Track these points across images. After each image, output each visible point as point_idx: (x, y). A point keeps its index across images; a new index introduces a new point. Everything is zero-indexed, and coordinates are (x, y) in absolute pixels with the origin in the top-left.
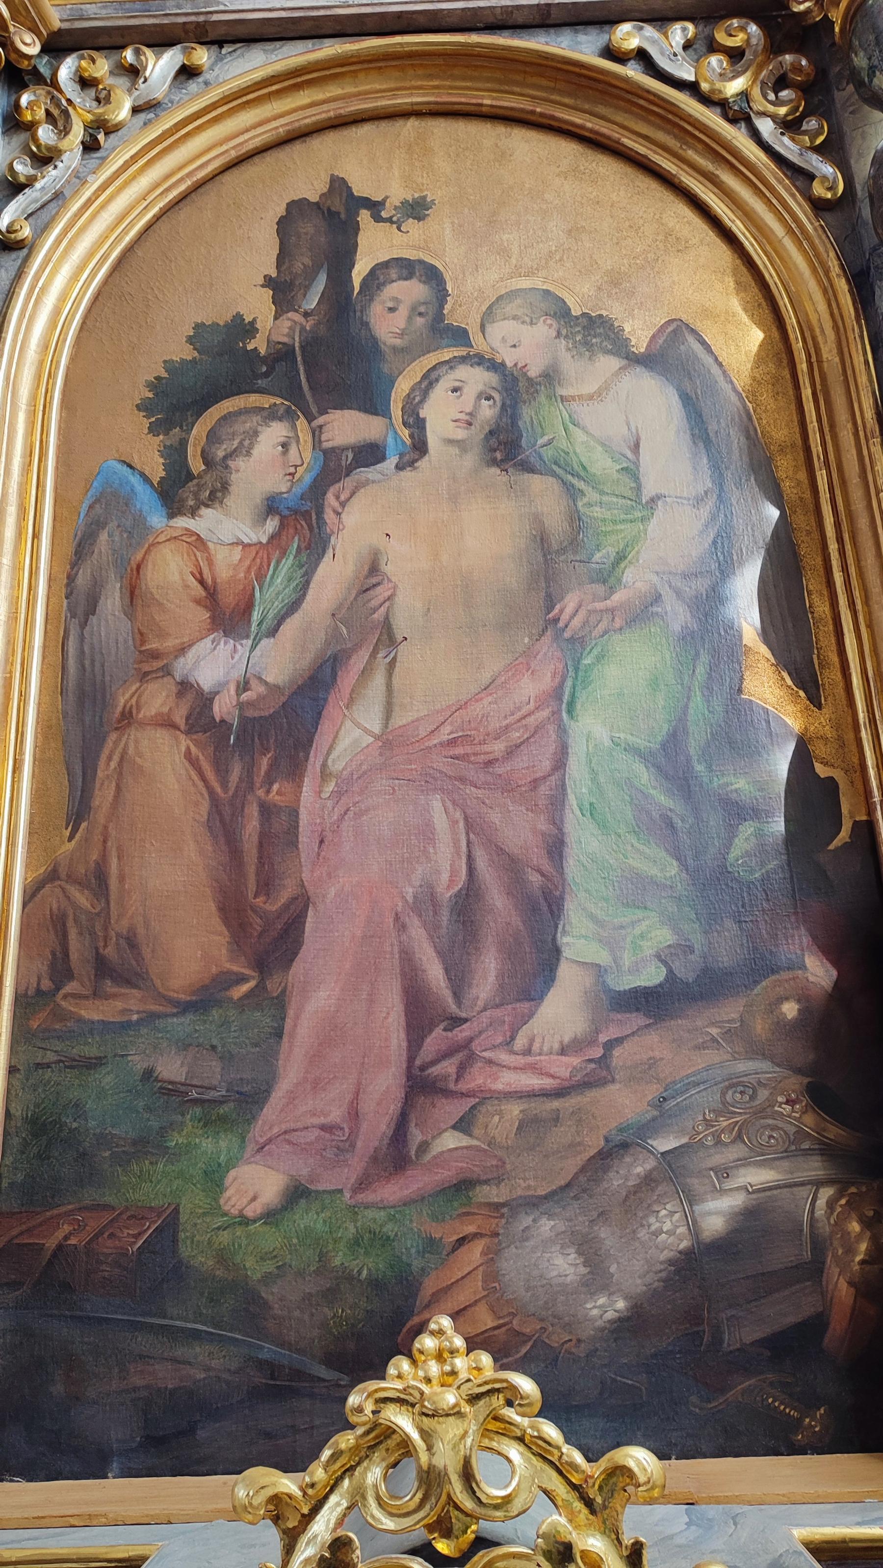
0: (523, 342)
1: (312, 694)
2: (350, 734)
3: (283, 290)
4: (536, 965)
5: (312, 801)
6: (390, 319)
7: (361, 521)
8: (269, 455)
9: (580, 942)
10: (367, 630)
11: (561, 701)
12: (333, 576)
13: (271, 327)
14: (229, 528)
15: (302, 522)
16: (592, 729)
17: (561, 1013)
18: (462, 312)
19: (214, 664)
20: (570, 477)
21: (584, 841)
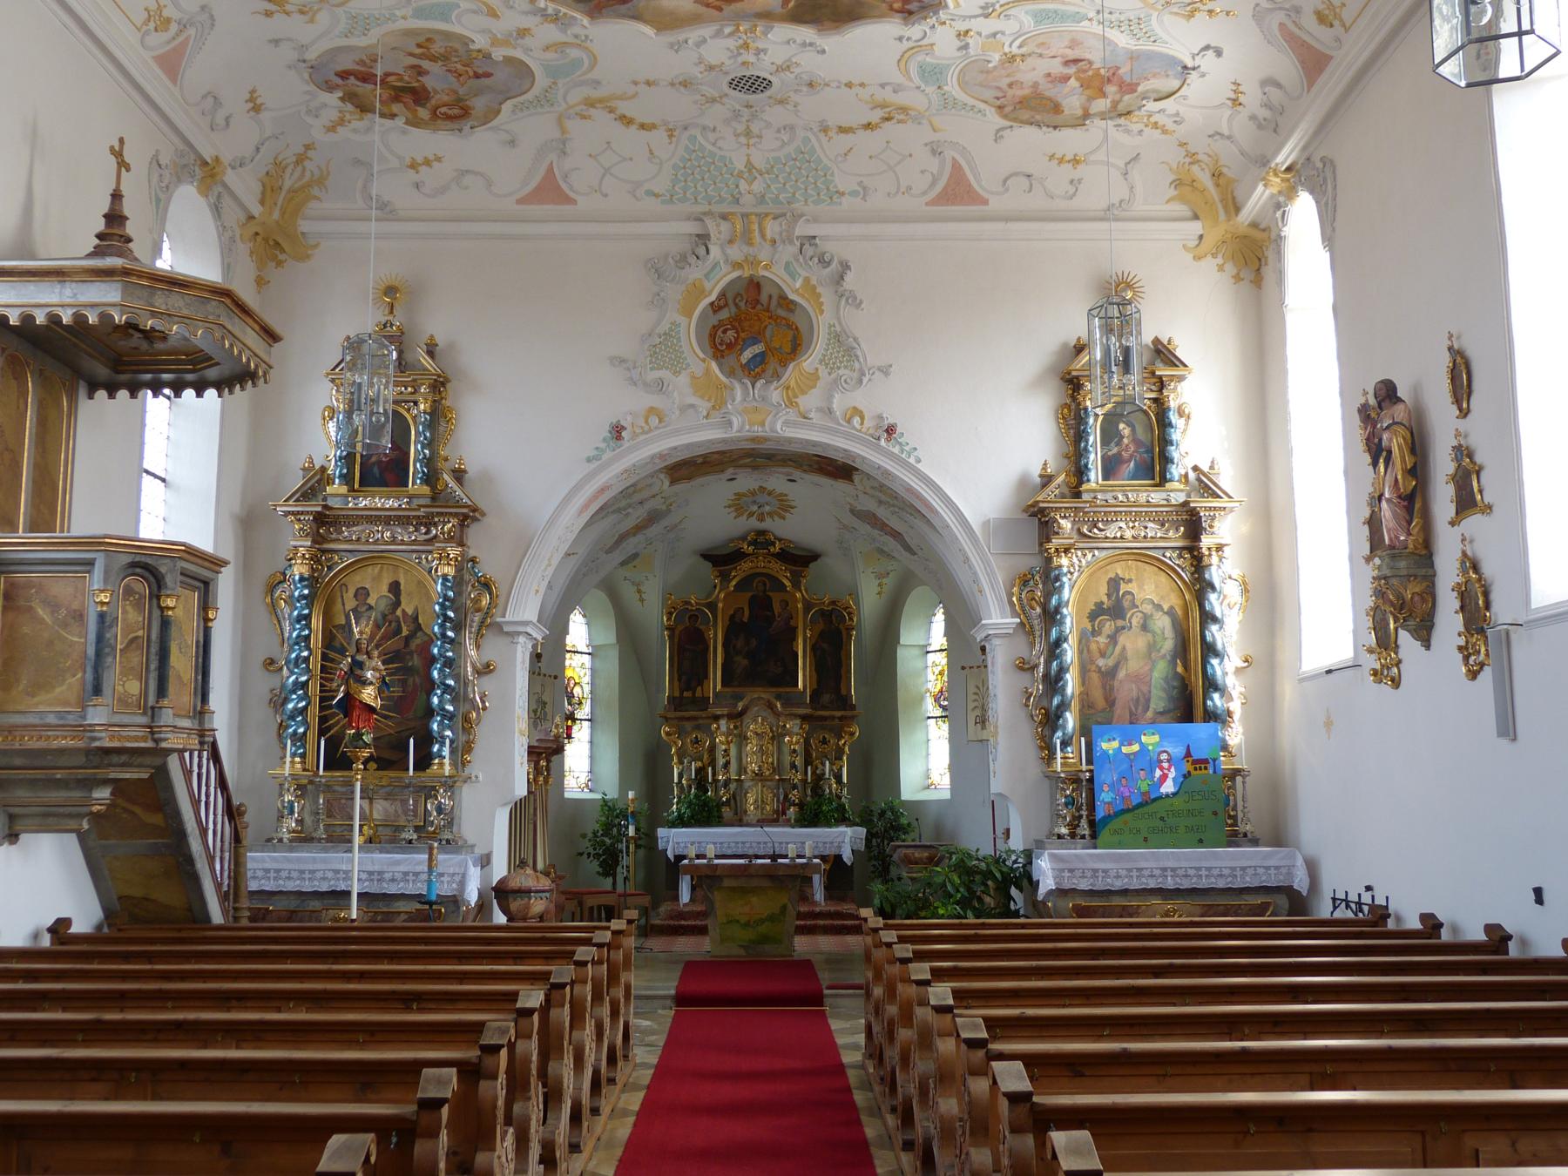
0: (1147, 608)
1: (1116, 667)
2: (1121, 674)
3: (1109, 596)
4: (1147, 709)
5: (1116, 683)
6: (1126, 604)
7: (1123, 639)
8: (1109, 627)
9: (1152, 705)
10: (1123, 658)
11: (1151, 670)
12: (1118, 649)
14: (1102, 640)
15: (1113, 639)
16: (1156, 674)
18: (1138, 602)
19: (1101, 662)
20: (1154, 633)
21: (1154, 691)
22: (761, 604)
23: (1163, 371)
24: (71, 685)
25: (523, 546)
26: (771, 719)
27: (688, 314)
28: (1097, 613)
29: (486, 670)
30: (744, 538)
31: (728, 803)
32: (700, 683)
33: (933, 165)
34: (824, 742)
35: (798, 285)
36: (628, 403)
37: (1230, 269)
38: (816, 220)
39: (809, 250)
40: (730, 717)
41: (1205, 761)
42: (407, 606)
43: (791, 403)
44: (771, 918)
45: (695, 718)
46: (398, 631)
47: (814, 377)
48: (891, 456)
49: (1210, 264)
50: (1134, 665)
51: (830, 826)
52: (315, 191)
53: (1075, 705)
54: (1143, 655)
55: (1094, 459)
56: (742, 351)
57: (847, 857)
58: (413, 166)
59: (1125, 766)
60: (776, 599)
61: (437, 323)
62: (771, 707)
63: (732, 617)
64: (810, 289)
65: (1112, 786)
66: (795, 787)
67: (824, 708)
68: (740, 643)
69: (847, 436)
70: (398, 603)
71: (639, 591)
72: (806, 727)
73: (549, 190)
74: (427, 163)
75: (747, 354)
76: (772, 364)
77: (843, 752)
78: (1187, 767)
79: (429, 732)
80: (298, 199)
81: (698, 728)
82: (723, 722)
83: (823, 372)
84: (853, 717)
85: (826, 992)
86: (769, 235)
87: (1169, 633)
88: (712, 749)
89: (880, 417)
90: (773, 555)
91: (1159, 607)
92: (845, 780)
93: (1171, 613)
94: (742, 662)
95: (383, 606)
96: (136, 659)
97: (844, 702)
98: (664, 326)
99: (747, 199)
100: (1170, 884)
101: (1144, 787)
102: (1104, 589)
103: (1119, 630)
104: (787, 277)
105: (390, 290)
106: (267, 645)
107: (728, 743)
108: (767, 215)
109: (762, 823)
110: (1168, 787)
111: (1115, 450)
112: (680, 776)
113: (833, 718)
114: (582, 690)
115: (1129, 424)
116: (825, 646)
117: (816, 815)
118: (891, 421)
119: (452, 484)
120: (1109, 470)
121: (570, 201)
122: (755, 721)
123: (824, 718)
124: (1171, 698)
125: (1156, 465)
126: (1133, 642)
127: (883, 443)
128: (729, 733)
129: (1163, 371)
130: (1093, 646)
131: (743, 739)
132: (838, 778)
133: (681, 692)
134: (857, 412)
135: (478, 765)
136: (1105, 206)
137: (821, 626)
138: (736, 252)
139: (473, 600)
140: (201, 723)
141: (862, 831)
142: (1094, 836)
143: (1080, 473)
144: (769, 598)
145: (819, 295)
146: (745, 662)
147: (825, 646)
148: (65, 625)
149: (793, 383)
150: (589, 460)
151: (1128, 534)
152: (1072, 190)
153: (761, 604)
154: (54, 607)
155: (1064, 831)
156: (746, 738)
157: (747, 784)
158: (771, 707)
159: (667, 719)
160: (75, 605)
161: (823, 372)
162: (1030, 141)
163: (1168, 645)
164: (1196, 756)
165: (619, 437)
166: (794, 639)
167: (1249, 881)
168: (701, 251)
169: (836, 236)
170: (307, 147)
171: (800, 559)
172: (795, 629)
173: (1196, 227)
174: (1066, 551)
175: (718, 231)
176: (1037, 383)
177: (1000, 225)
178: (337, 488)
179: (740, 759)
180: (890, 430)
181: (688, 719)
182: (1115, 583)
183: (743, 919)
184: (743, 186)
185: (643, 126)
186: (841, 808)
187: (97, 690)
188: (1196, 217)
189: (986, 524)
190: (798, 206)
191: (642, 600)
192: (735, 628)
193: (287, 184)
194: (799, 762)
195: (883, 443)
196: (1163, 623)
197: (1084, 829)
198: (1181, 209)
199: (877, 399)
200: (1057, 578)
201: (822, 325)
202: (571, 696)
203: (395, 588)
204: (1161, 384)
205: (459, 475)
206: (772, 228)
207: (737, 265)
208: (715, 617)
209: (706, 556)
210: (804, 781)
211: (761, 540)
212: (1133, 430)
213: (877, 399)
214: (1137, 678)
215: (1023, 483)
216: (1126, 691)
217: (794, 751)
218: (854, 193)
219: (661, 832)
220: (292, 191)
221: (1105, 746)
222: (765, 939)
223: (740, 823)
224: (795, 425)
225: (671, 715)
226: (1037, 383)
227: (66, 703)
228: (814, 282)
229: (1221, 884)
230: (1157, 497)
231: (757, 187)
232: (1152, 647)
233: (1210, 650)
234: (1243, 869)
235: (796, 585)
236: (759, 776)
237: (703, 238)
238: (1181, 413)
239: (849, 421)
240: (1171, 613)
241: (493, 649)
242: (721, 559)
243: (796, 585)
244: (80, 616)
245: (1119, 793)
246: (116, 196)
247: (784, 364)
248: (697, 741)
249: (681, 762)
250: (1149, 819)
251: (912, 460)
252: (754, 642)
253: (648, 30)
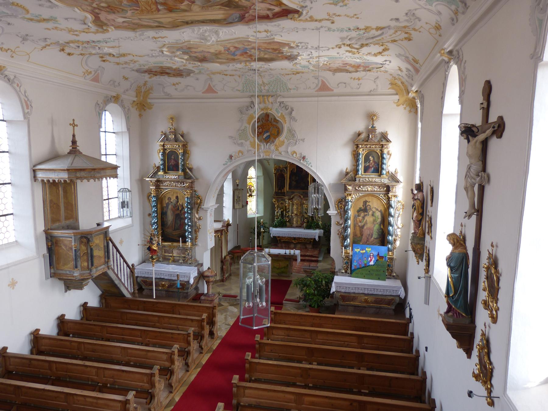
0: (374, 210)
2: (365, 227)
6: (368, 208)
7: (366, 218)
8: (362, 215)
9: (373, 236)
10: (366, 223)
12: (365, 220)
13: (363, 208)
14: (360, 218)
15: (364, 218)
16: (375, 228)
17: (372, 239)
19: (360, 224)
20: (375, 217)
23: (384, 143)
24: (72, 264)
25: (208, 187)
26: (300, 200)
27: (249, 123)
28: (360, 211)
29: (200, 219)
33: (316, 81)
35: (279, 115)
36: (234, 149)
37: (408, 109)
38: (283, 97)
39: (282, 105)
40: (289, 199)
41: (383, 257)
42: (180, 202)
43: (277, 150)
44: (284, 267)
46: (178, 209)
47: (283, 142)
48: (303, 165)
49: (402, 107)
50: (369, 225)
52: (151, 91)
53: (351, 236)
54: (371, 223)
55: (361, 168)
56: (264, 135)
57: (317, 239)
58: (174, 85)
59: (361, 256)
61: (184, 128)
62: (300, 197)
63: (292, 171)
64: (283, 116)
65: (357, 261)
69: (292, 159)
70: (178, 202)
73: (210, 90)
74: (177, 84)
75: (265, 136)
76: (272, 139)
78: (378, 258)
79: (185, 236)
80: (147, 93)
81: (282, 200)
83: (286, 141)
85: (284, 302)
86: (270, 101)
87: (380, 217)
89: (301, 154)
91: (377, 210)
93: (381, 211)
95: (174, 202)
96: (85, 257)
98: (243, 128)
99: (264, 91)
100: (366, 292)
101: (365, 262)
102: (362, 204)
103: (365, 215)
104: (276, 113)
105: (172, 118)
106: (149, 210)
108: (269, 96)
109: (297, 227)
110: (372, 263)
111: (368, 164)
112: (277, 213)
114: (254, 188)
115: (373, 157)
118: (304, 155)
119: (189, 172)
120: (366, 170)
121: (215, 92)
124: (379, 235)
125: (378, 169)
126: (369, 219)
127: (302, 161)
129: (384, 143)
130: (358, 220)
131: (293, 204)
134: (295, 152)
135: (199, 242)
136: (369, 91)
138: (262, 106)
139: (196, 203)
140: (108, 264)
141: (322, 231)
142: (351, 273)
143: (356, 171)
145: (285, 118)
148: (68, 251)
149: (277, 144)
150: (224, 165)
151: (369, 189)
152: (358, 87)
154: (66, 246)
155: (343, 271)
158: (300, 197)
160: (70, 246)
161: (286, 141)
162: (341, 76)
163: (379, 220)
164: (380, 255)
165: (231, 159)
167: (388, 293)
168: (252, 106)
169: (288, 101)
170: (146, 82)
173: (397, 97)
174: (350, 195)
175: (256, 101)
176: (346, 144)
177: (337, 98)
178: (161, 173)
180: (304, 158)
182: (365, 202)
183: (278, 267)
184: (262, 88)
185: (230, 75)
187: (76, 267)
188: (397, 94)
189: (330, 184)
190: (279, 93)
193: (143, 90)
195: (302, 161)
196: (378, 214)
197: (349, 271)
198: (392, 91)
199: (301, 149)
200: (347, 202)
201: (286, 127)
202: (250, 190)
203: (177, 197)
204: (382, 146)
205: (191, 169)
206: (271, 99)
207: (262, 110)
212: (374, 159)
213: (301, 149)
214: (369, 229)
215: (341, 173)
216: (366, 232)
218: (294, 89)
219: (271, 228)
220: (145, 92)
221: (356, 250)
222: (283, 272)
223: (291, 227)
224: (278, 156)
225: (275, 197)
226: (346, 144)
227: (71, 268)
228: (284, 114)
229: (380, 293)
230: (378, 180)
231: (267, 88)
232: (374, 221)
233: (389, 224)
234: (387, 290)
236: (296, 215)
237: (252, 103)
238: (388, 153)
239: (293, 155)
240: (381, 211)
241: (201, 213)
244: (72, 249)
245: (358, 263)
246: (74, 136)
247: (275, 138)
250: (364, 271)
251: (310, 166)
252: (297, 178)
253: (218, 65)
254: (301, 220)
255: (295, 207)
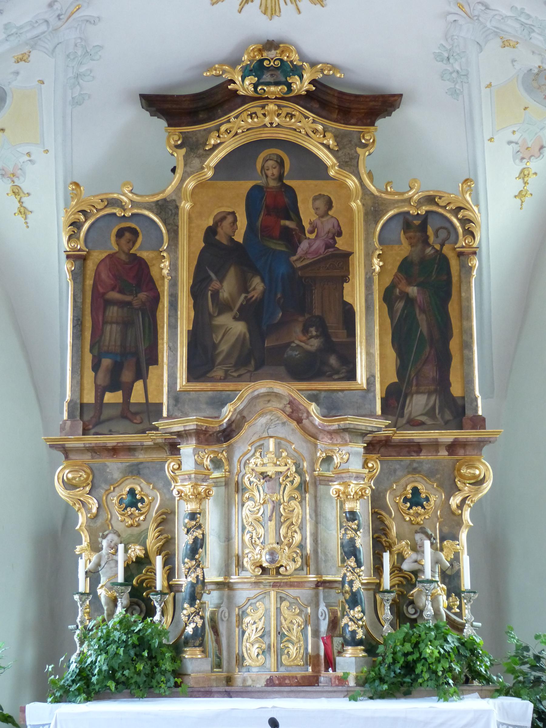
22: (273, 207)
26: (298, 443)
30: (234, 63)
31: (199, 633)
32: (141, 374)
34: (416, 499)
45: (130, 449)
51: (440, 691)
60: (305, 192)
62: (296, 415)
63: (211, 232)
66: (354, 600)
67: (414, 424)
68: (228, 287)
71: (17, 191)
72: (375, 465)
77: (459, 523)
81: (135, 471)
82: (187, 450)
84: (480, 444)
88: (166, 519)
90: (299, 99)
92: (466, 583)
94: (232, 329)
97: (457, 412)
107: (200, 498)
109: (278, 685)
112: (93, 576)
113: (435, 445)
116: (413, 291)
117: (409, 668)
122: (261, 448)
123: (416, 448)
128: (201, 475)
131: (235, 488)
132: (450, 578)
133: (100, 394)
137: (403, 249)
144: (291, 192)
146: (239, 328)
147: (413, 291)
153: (273, 207)
156: (240, 488)
157: (243, 595)
159: (66, 452)
166: (344, 277)
171: (355, 108)
172: (346, 256)
179: (228, 539)
181: (114, 451)
186: (468, 651)
191: (24, 212)
192: (216, 255)
194: (363, 542)
208: (174, 232)
209: (157, 103)
210: (376, 588)
211: (271, 65)
217: (352, 516)
223: (228, 687)
225: (77, 441)
235: (349, 163)
242: (185, 109)
243: (349, 163)
248: (133, 501)
249: (95, 547)
254: (311, 620)
255: (247, 511)
